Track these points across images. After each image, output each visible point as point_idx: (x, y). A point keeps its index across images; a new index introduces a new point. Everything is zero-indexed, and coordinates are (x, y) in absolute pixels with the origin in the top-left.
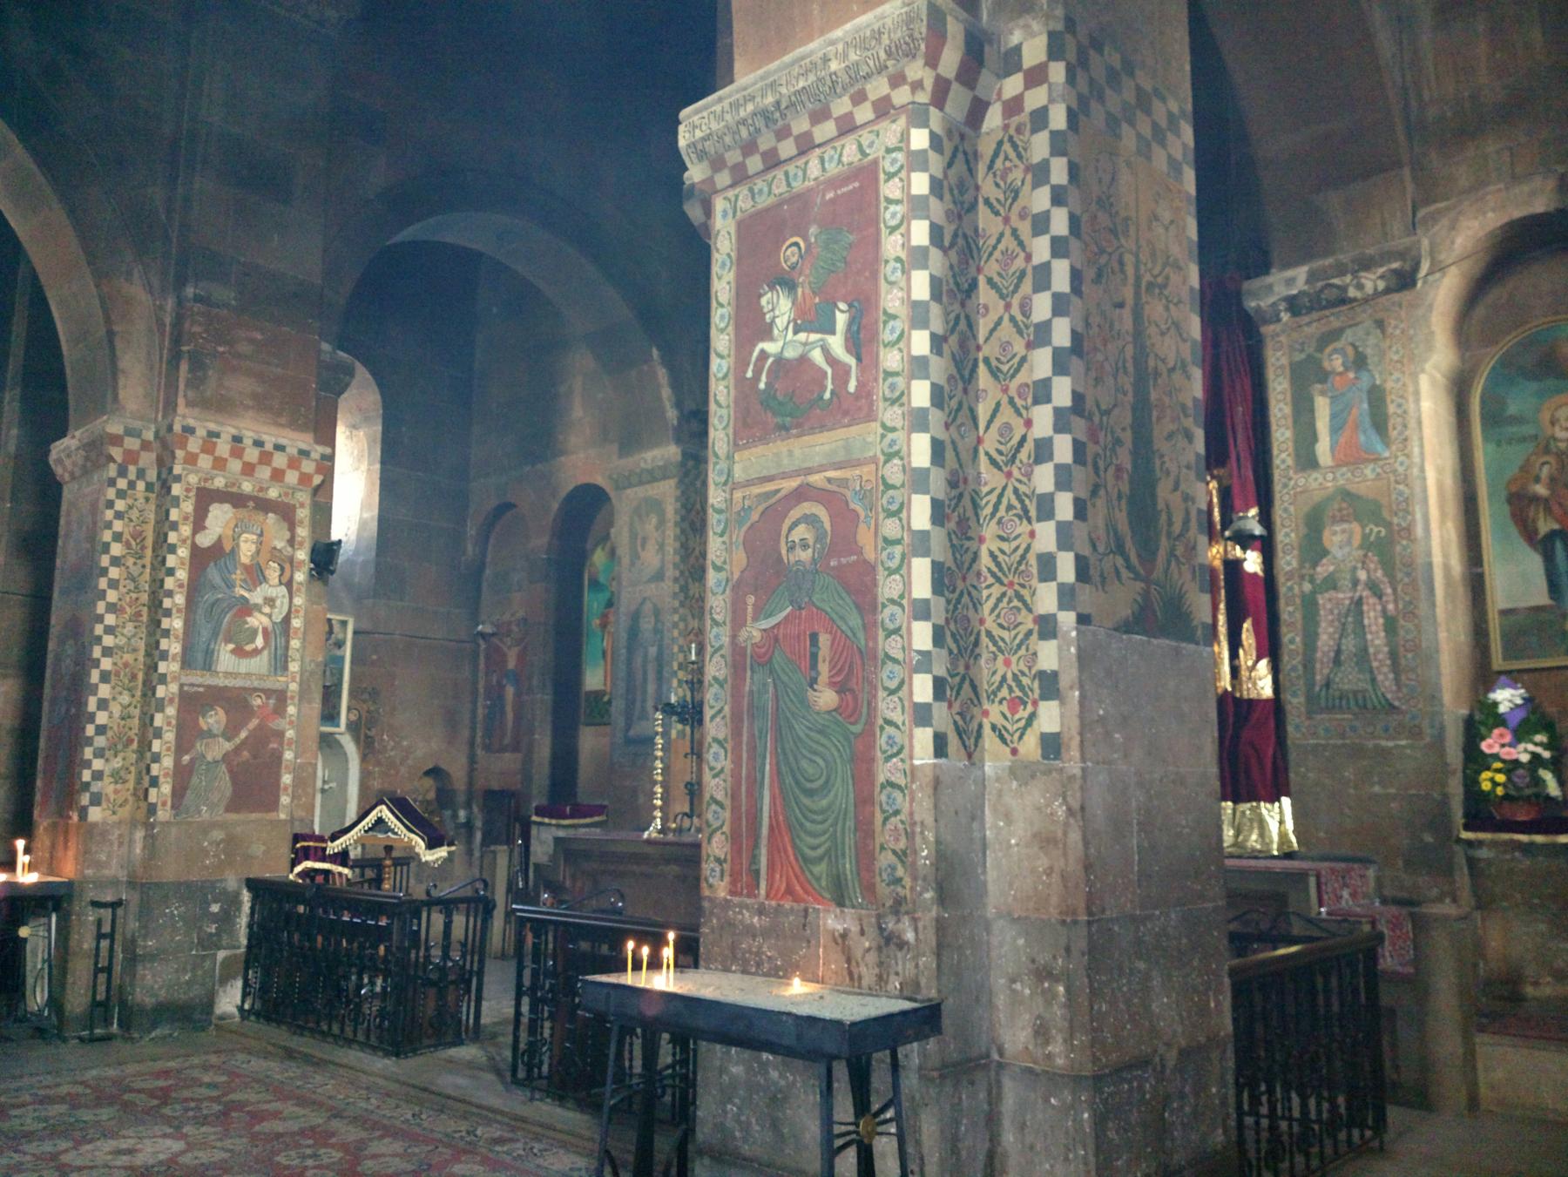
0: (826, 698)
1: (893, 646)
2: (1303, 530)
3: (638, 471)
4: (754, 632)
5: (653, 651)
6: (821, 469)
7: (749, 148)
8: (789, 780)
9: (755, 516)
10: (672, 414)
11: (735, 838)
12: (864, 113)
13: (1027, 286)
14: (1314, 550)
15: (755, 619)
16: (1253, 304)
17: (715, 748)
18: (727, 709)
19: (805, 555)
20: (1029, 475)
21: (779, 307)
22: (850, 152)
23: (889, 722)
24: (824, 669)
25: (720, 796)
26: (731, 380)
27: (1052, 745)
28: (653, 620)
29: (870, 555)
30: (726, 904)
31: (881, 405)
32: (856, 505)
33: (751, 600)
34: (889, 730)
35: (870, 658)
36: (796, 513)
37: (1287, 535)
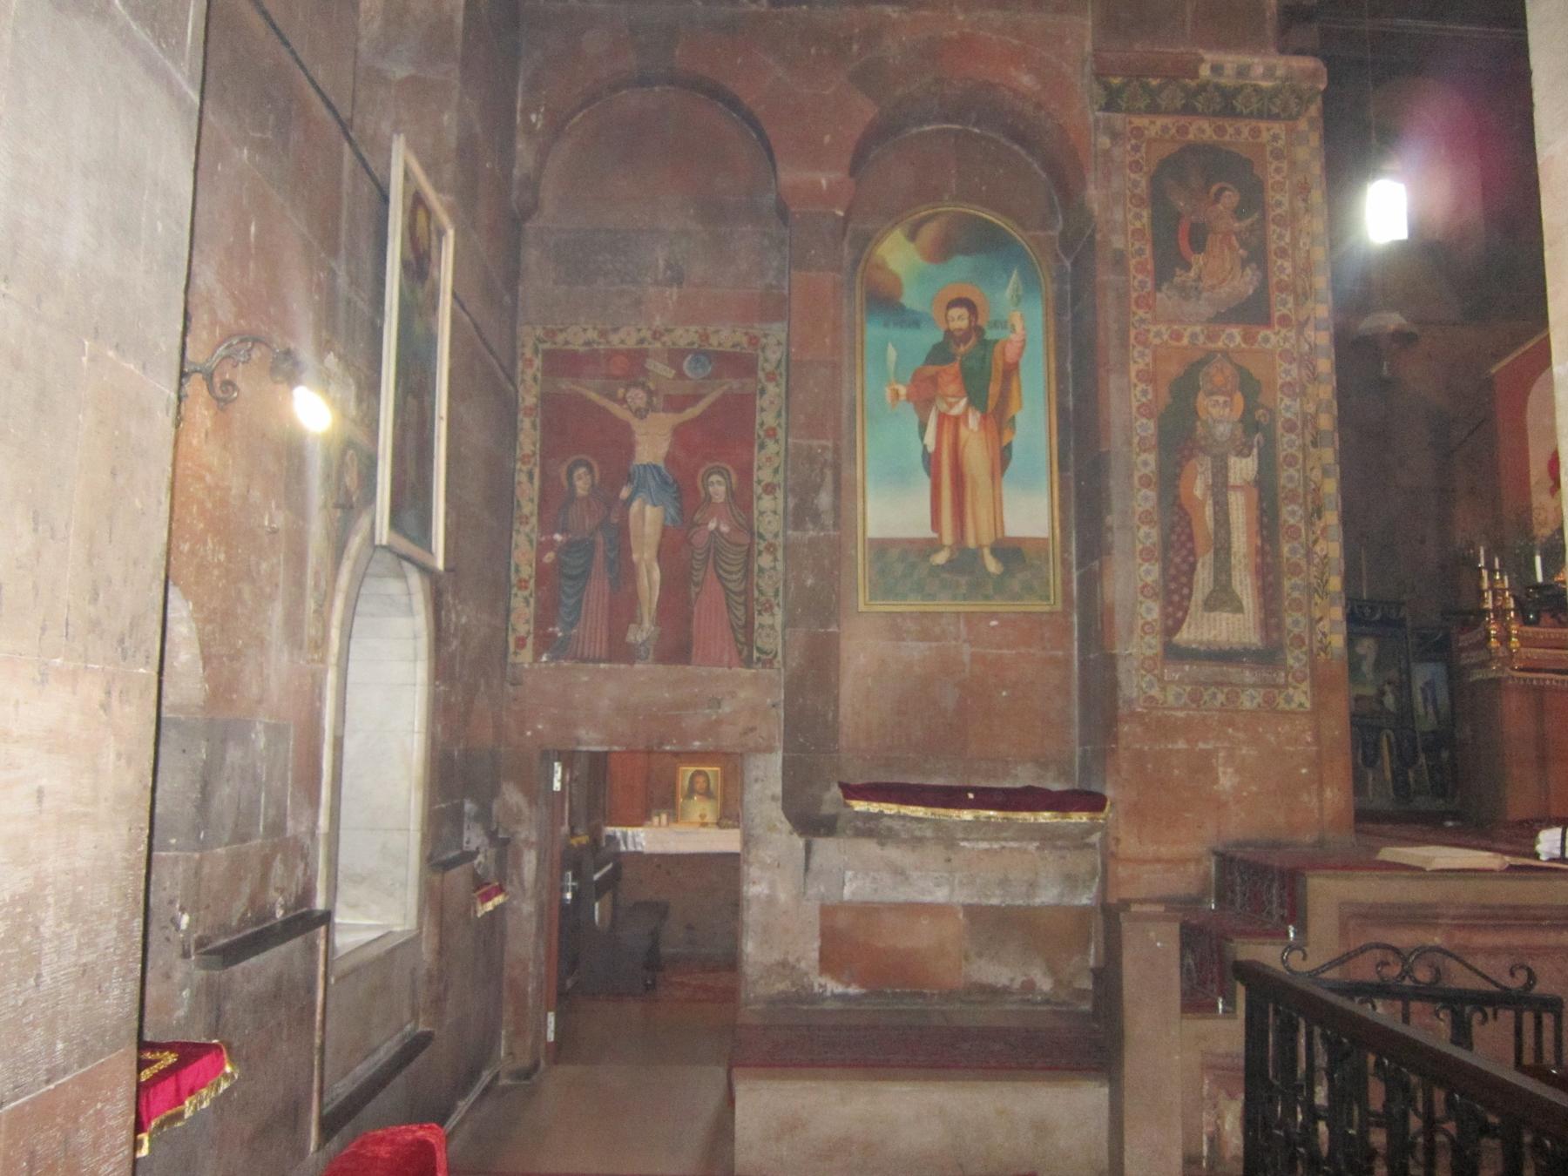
3: (1193, 84)
5: (1243, 468)
28: (1238, 398)
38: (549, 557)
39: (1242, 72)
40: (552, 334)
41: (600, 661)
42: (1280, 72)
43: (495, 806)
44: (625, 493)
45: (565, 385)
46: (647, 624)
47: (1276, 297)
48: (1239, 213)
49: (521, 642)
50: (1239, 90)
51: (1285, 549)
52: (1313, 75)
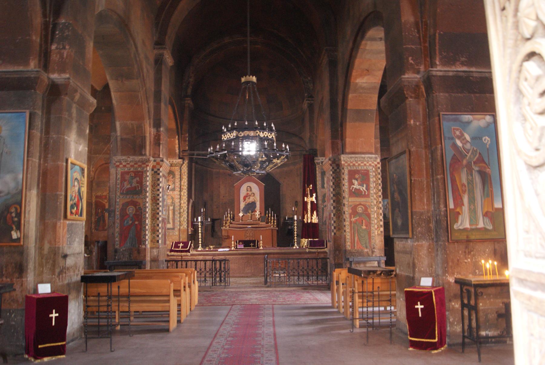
0: (364, 227)
1: (373, 222)
2: (322, 198)
4: (353, 219)
5: (171, 208)
6: (362, 202)
7: (352, 162)
8: (359, 236)
9: (353, 206)
10: (177, 151)
11: (351, 243)
12: (368, 164)
13: (378, 185)
14: (324, 201)
15: (353, 218)
16: (317, 161)
17: (348, 233)
18: (349, 228)
19: (361, 211)
20: (379, 205)
21: (356, 182)
22: (365, 168)
23: (373, 230)
24: (364, 224)
25: (349, 238)
26: (348, 189)
27: (381, 232)
28: (171, 200)
29: (370, 212)
30: (351, 250)
31: (370, 196)
32: (367, 207)
33: (352, 216)
34: (373, 231)
35: (370, 223)
36: (359, 206)
37: (320, 198)
38: (96, 219)
39: (173, 161)
40: (96, 194)
41: (101, 231)
42: (177, 162)
43: (90, 247)
44: (104, 212)
45: (98, 199)
46: (107, 227)
47: (176, 188)
48: (172, 178)
49: (93, 229)
50: (172, 164)
51: (176, 217)
52: (181, 162)
